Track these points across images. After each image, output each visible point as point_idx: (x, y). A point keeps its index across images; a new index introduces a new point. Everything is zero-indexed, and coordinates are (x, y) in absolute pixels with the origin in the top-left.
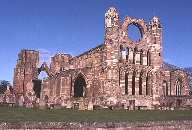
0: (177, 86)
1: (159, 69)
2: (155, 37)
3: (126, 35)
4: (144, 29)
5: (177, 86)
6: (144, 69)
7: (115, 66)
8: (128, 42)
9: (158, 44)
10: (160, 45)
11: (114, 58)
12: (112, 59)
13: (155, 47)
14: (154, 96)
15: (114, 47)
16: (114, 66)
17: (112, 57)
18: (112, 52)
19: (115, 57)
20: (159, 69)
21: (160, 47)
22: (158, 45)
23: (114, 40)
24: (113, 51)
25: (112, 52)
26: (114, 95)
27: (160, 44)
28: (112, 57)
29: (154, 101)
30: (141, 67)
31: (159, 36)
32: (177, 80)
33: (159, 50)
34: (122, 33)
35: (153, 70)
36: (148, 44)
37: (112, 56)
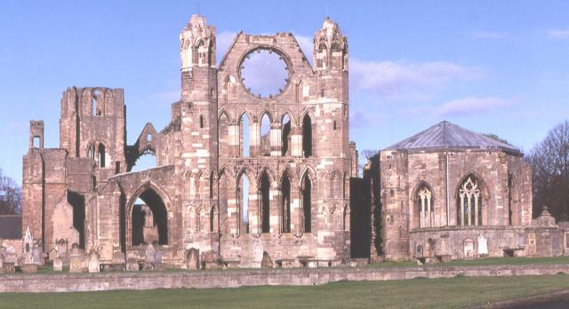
0: (469, 197)
1: (332, 163)
2: (323, 78)
3: (238, 84)
4: (293, 60)
5: (469, 197)
6: (293, 165)
7: (203, 166)
8: (245, 100)
9: (329, 97)
10: (336, 100)
11: (199, 148)
12: (194, 150)
13: (321, 105)
14: (321, 235)
15: (199, 121)
16: (200, 166)
17: (195, 145)
18: (194, 134)
19: (201, 145)
20: (332, 163)
21: (334, 107)
22: (329, 100)
23: (199, 103)
24: (197, 131)
25: (194, 134)
26: (200, 237)
27: (337, 97)
28: (195, 145)
29: (321, 246)
30: (282, 161)
31: (332, 75)
32: (469, 179)
33: (333, 114)
34: (228, 80)
35: (318, 167)
36: (306, 99)
37: (194, 142)
